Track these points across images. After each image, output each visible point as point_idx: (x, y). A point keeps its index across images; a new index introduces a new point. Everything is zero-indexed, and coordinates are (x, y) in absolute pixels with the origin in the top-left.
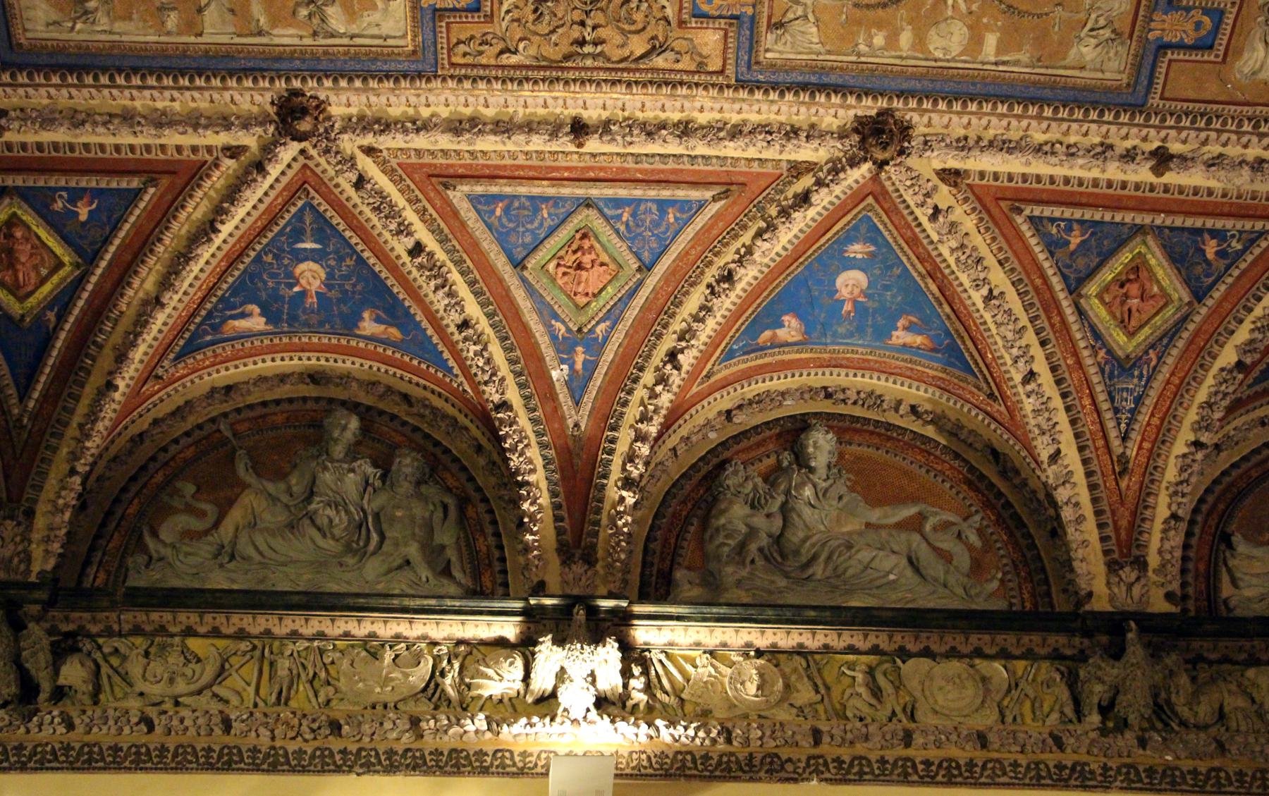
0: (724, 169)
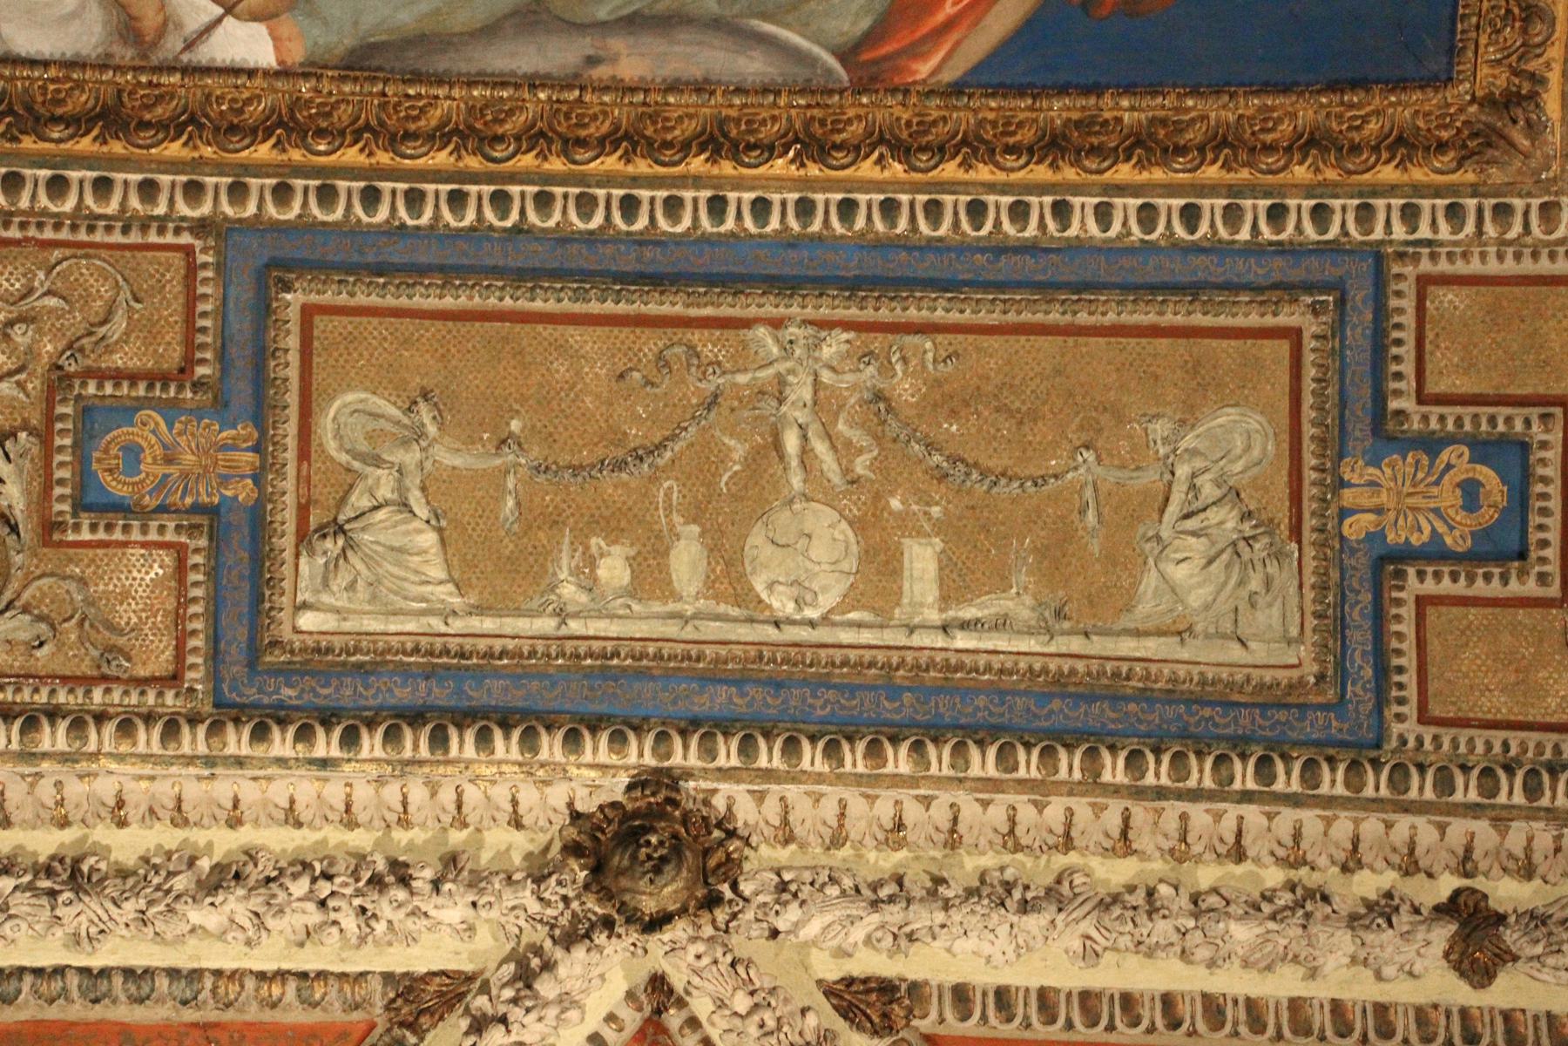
0: (189, 1015)
